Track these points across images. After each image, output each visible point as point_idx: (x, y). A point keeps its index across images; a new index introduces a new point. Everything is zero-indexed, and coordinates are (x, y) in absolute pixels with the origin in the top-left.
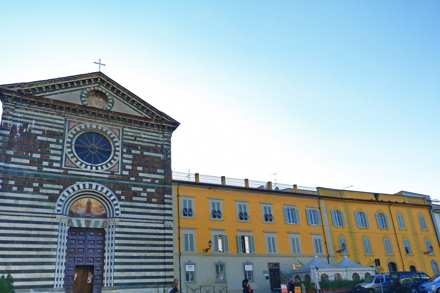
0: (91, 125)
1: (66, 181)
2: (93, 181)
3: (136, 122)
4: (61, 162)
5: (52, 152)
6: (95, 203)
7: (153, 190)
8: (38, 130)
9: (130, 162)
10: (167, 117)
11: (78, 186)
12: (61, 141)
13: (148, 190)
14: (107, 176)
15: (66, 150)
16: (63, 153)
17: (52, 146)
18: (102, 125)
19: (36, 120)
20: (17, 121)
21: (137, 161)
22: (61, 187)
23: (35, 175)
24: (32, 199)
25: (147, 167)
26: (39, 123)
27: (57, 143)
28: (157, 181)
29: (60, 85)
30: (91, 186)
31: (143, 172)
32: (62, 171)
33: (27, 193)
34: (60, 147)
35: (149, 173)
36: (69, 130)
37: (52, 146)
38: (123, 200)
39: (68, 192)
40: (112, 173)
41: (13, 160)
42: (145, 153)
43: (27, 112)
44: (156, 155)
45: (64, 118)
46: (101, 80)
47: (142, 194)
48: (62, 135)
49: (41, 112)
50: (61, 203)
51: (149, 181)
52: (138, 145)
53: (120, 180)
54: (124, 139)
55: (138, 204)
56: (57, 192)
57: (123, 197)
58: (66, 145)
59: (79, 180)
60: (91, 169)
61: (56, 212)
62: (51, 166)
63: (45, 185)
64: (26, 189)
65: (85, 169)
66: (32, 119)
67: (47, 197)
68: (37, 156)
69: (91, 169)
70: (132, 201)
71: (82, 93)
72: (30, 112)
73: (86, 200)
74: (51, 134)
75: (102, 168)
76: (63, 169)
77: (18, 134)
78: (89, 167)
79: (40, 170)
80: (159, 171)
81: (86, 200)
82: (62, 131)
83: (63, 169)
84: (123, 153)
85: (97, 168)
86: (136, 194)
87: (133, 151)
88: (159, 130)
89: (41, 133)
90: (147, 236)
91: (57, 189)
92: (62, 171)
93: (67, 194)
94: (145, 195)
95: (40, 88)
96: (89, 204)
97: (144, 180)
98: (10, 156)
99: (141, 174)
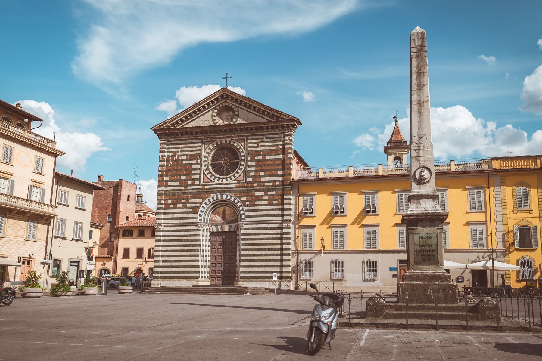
0: (221, 141)
1: (203, 194)
2: (224, 192)
3: (257, 129)
4: (199, 179)
5: (194, 172)
6: (229, 210)
7: (274, 193)
8: (183, 155)
9: (253, 169)
10: (286, 115)
11: (213, 198)
12: (199, 161)
13: (269, 193)
14: (234, 185)
15: (204, 168)
16: (201, 172)
17: (193, 167)
18: (230, 139)
19: (182, 148)
20: (169, 152)
21: (260, 166)
22: (201, 200)
23: (184, 194)
24: (183, 213)
25: (268, 170)
26: (184, 149)
27: (197, 164)
28: (278, 183)
29: (195, 112)
30: (222, 195)
31: (265, 176)
32: (201, 187)
33: (178, 208)
34: (198, 167)
35: (270, 176)
36: (205, 150)
37: (193, 167)
38: (247, 206)
39: (206, 204)
40: (239, 182)
41: (169, 184)
42: (267, 157)
43: (175, 142)
44: (277, 157)
45: (200, 141)
46: (227, 95)
47: (264, 198)
48: (200, 155)
49: (184, 140)
50: (201, 214)
51: (270, 184)
52: (261, 150)
53: (245, 187)
54: (248, 147)
55: (260, 208)
56: (198, 205)
57: (247, 203)
58: (203, 164)
59: (213, 192)
60: (222, 181)
61: (198, 221)
62: (193, 185)
63: (190, 201)
64: (178, 206)
65: (218, 182)
66: (178, 148)
67: (191, 210)
68: (183, 177)
69: (222, 181)
70: (255, 205)
71: (213, 112)
72: (177, 142)
73: (222, 208)
74: (192, 157)
75: (231, 179)
76: (201, 185)
77: (171, 162)
78: (221, 180)
79: (186, 189)
80: (280, 172)
81: (222, 208)
82: (199, 152)
83: (201, 185)
84: (247, 161)
85: (227, 180)
86: (259, 198)
87: (256, 158)
88: (280, 131)
89: (185, 157)
90: (267, 236)
91: (198, 203)
92: (201, 187)
93: (205, 206)
94: (266, 198)
95: (181, 120)
96: (224, 211)
97: (266, 184)
98: (167, 181)
99: (263, 179)
